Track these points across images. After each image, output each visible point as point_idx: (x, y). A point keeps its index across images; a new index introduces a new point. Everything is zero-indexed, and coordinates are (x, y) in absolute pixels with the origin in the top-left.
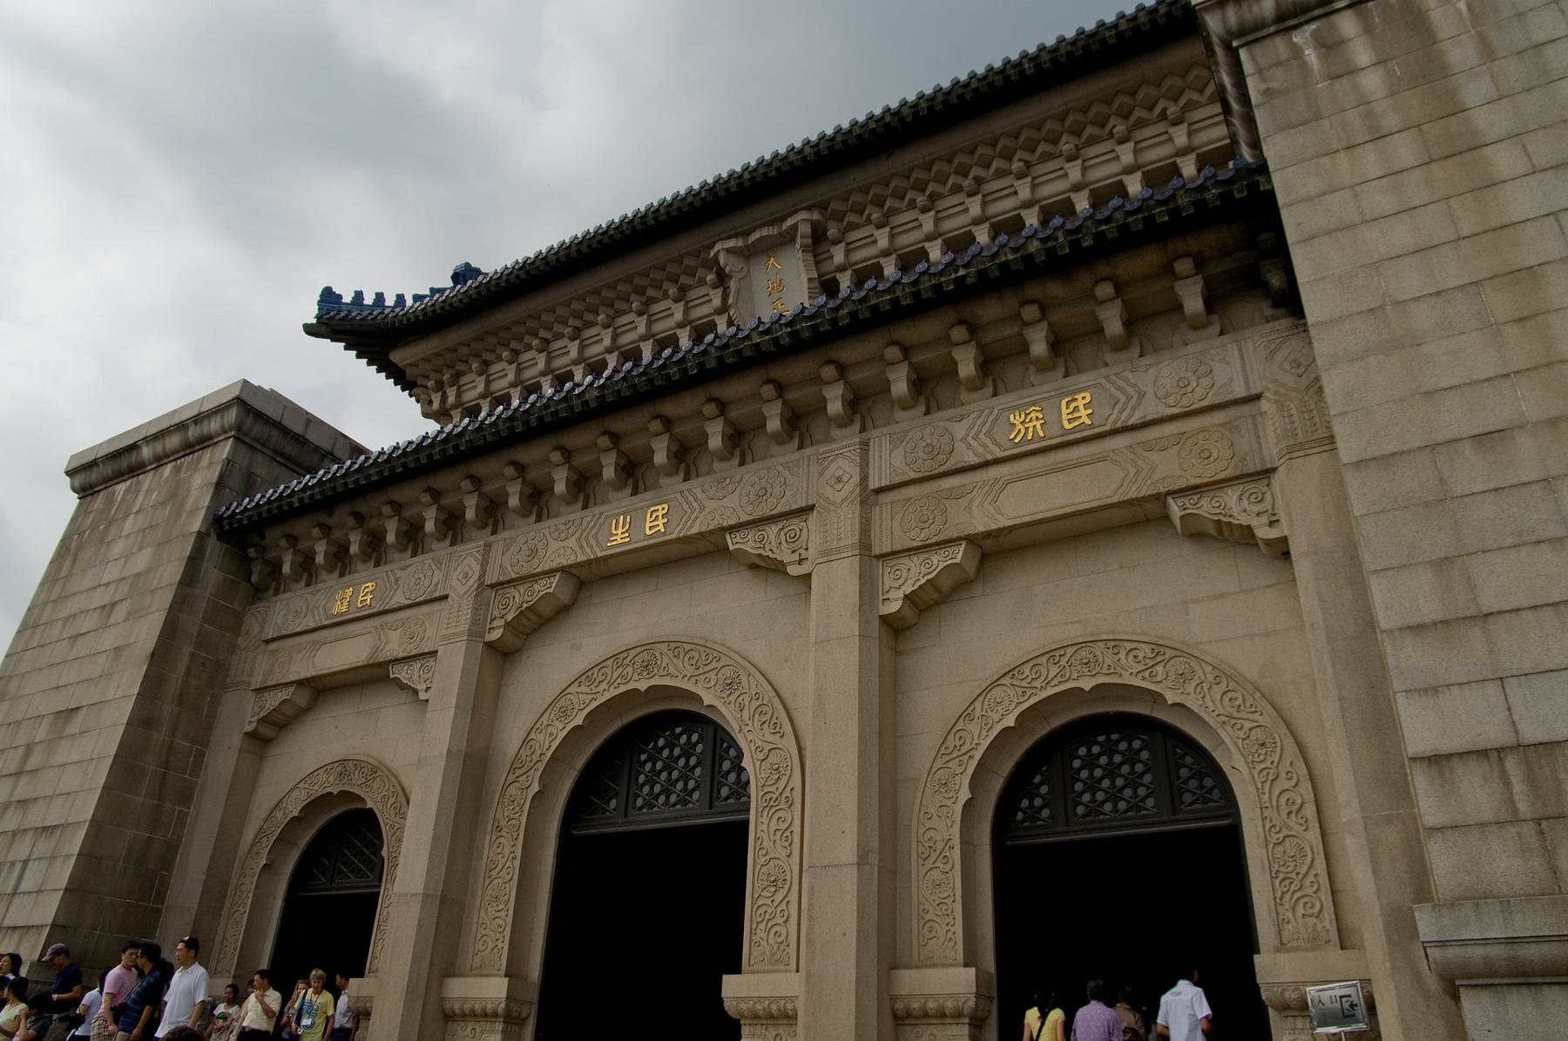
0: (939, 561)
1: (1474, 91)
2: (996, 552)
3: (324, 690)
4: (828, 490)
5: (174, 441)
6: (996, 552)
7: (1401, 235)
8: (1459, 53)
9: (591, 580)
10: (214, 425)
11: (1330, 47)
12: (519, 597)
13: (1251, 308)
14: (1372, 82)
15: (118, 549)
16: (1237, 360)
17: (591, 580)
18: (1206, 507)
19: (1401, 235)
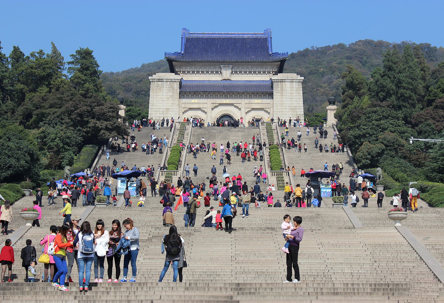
0: (250, 109)
1: (284, 92)
2: (253, 109)
3: (191, 109)
4: (243, 103)
5: (170, 80)
6: (253, 109)
7: (278, 100)
8: (284, 89)
9: (221, 104)
10: (177, 80)
11: (278, 85)
12: (215, 105)
13: (270, 97)
14: (280, 89)
15: (165, 91)
16: (269, 101)
17: (221, 104)
18: (266, 109)
19: (278, 100)
